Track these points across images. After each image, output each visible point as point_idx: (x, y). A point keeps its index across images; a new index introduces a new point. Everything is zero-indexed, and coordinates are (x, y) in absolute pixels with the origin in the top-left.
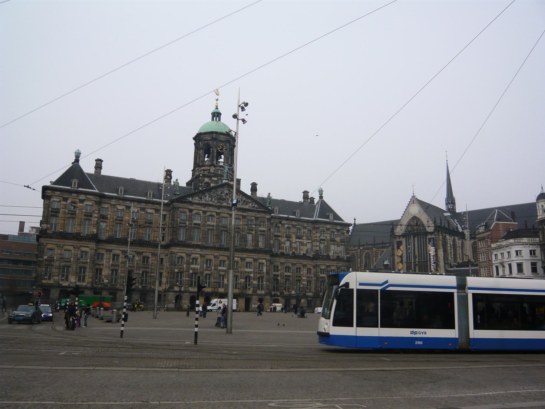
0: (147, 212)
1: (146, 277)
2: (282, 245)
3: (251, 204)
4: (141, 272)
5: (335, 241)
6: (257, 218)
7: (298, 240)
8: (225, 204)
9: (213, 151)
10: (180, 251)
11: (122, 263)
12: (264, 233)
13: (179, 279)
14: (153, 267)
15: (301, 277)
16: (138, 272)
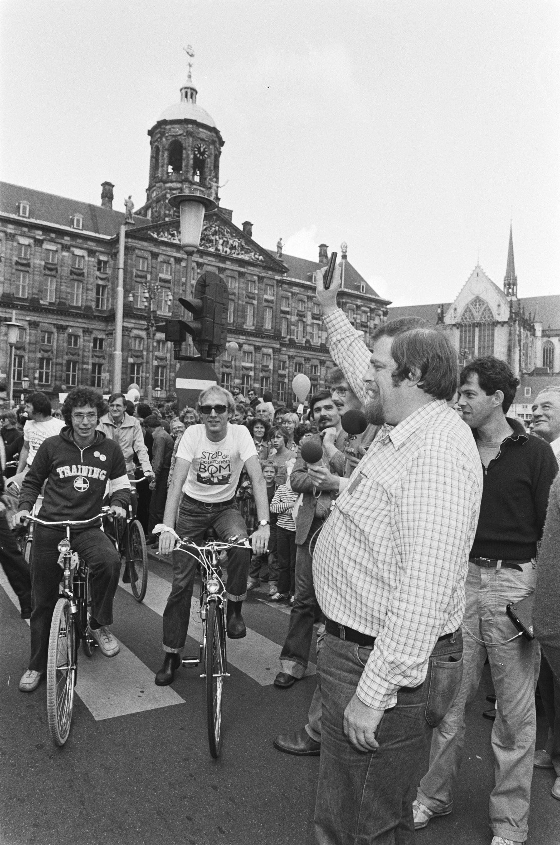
0: (73, 254)
1: (74, 371)
2: (292, 327)
3: (253, 254)
4: (65, 362)
5: (366, 327)
6: (261, 279)
7: (315, 321)
8: (212, 250)
9: (188, 156)
10: (137, 326)
11: (30, 343)
12: (271, 305)
13: (135, 375)
14: (86, 354)
15: (317, 380)
16: (59, 360)
